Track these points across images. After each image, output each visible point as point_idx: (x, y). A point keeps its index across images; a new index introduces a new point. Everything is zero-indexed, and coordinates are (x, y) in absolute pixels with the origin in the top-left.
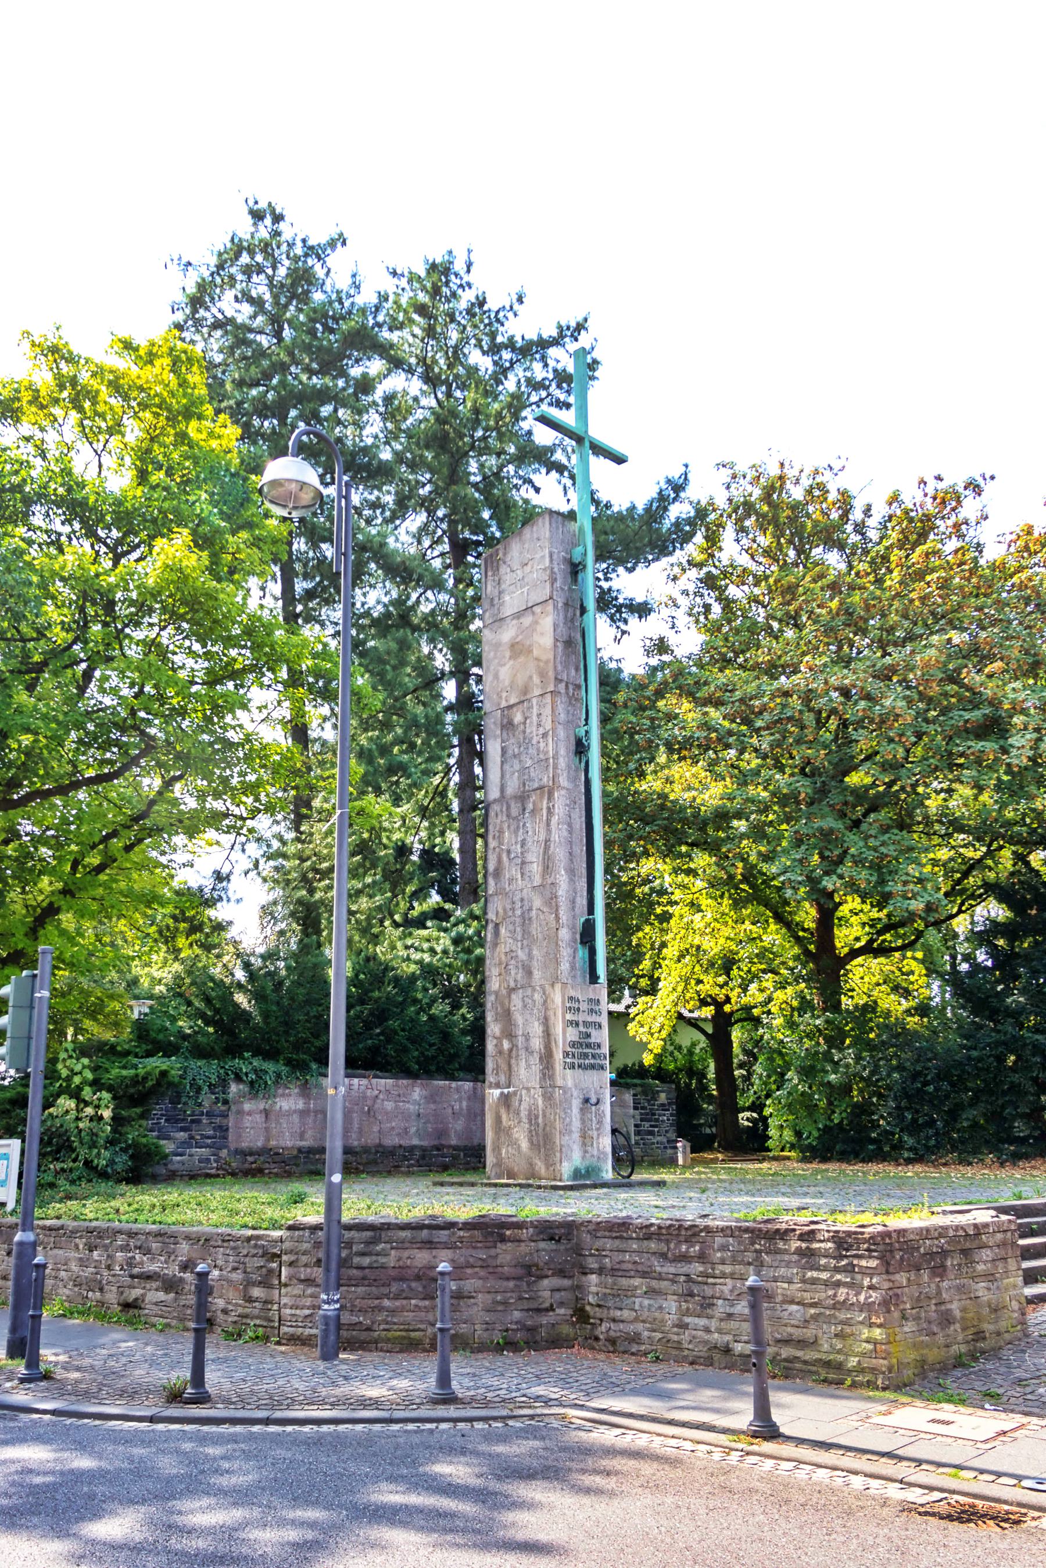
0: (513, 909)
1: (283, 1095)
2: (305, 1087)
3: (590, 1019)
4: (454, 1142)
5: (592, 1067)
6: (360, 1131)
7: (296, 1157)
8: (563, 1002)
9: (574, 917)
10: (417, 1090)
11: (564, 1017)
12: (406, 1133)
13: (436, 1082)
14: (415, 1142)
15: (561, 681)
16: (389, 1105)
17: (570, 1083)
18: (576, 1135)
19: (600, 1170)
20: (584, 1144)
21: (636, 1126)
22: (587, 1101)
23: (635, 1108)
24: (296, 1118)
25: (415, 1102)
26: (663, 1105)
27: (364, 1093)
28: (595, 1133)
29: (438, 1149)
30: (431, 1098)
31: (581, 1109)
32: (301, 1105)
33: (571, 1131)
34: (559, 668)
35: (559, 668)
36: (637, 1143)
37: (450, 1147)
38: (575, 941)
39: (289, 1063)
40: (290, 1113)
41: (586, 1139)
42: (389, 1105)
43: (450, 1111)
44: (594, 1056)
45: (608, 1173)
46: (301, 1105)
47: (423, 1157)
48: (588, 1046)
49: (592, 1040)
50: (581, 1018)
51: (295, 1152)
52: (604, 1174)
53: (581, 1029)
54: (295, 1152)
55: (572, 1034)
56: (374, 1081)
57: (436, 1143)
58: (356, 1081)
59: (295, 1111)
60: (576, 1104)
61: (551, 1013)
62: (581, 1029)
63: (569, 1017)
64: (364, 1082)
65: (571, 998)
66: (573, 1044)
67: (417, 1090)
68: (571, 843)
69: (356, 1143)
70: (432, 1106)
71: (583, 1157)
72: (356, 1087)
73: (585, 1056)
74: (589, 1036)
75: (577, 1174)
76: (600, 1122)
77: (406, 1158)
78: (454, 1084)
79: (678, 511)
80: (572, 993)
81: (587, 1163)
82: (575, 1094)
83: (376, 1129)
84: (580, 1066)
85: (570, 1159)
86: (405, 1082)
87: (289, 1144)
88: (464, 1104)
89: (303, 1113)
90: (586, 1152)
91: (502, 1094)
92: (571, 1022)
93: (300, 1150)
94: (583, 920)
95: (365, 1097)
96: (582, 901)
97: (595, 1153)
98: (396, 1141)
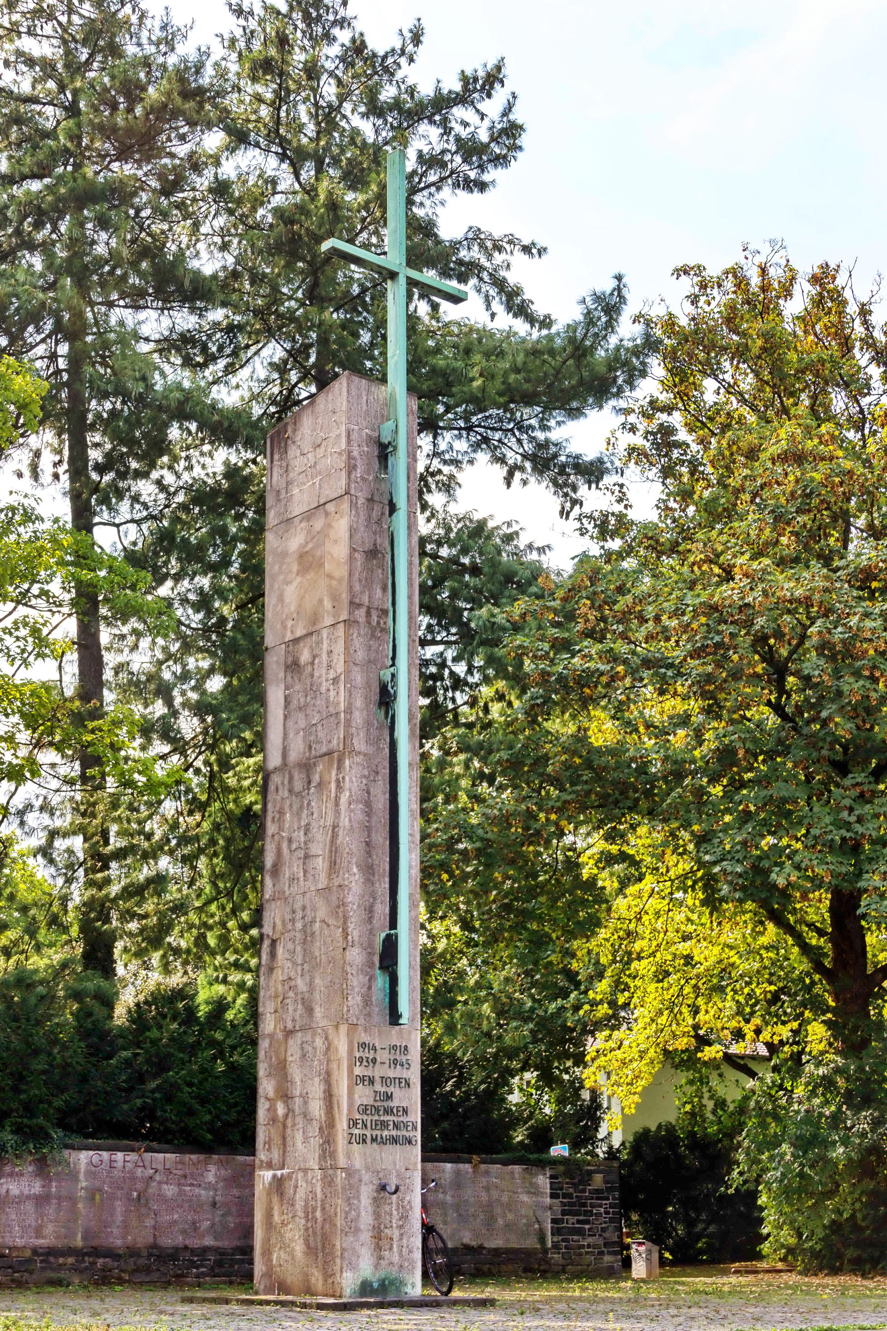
0: (293, 921)
1: (11, 1175)
2: (42, 1164)
3: (391, 1074)
5: (394, 1140)
6: (126, 1225)
7: (29, 1261)
8: (350, 1051)
9: (371, 932)
10: (213, 1168)
11: (350, 1071)
12: (196, 1229)
14: (209, 1241)
15: (359, 606)
16: (170, 1190)
17: (358, 1163)
18: (366, 1236)
19: (402, 1283)
20: (378, 1248)
21: (554, 1221)
22: (383, 1188)
23: (553, 1196)
24: (29, 1207)
25: (209, 1186)
26: (597, 1191)
27: (131, 1172)
28: (396, 1234)
31: (375, 1199)
32: (37, 1188)
33: (357, 1230)
34: (357, 587)
35: (357, 587)
36: (556, 1246)
38: (371, 965)
39: (18, 1130)
40: (21, 1199)
41: (379, 1239)
42: (170, 1190)
44: (396, 1126)
45: (415, 1287)
46: (37, 1188)
47: (219, 1264)
48: (388, 1111)
49: (395, 1103)
50: (378, 1072)
51: (28, 1253)
52: (409, 1289)
53: (378, 1087)
54: (28, 1253)
55: (364, 1095)
56: (148, 1156)
58: (120, 1156)
59: (28, 1197)
60: (366, 1194)
61: (334, 1066)
62: (378, 1087)
63: (358, 1071)
64: (133, 1157)
65: (363, 1045)
66: (365, 1109)
67: (213, 1168)
68: (369, 829)
69: (119, 1242)
70: (235, 1192)
71: (377, 1266)
72: (120, 1164)
73: (384, 1125)
74: (389, 1097)
75: (365, 1288)
76: (404, 1217)
77: (193, 1265)
79: (627, 331)
80: (365, 1038)
81: (382, 1274)
82: (366, 1177)
83: (149, 1222)
84: (374, 1140)
85: (353, 1267)
86: (194, 1157)
87: (19, 1242)
89: (41, 1200)
90: (380, 1258)
91: (274, 1176)
92: (363, 1079)
93: (35, 1251)
94: (383, 935)
95: (133, 1178)
96: (382, 909)
97: (396, 1259)
98: (180, 1240)
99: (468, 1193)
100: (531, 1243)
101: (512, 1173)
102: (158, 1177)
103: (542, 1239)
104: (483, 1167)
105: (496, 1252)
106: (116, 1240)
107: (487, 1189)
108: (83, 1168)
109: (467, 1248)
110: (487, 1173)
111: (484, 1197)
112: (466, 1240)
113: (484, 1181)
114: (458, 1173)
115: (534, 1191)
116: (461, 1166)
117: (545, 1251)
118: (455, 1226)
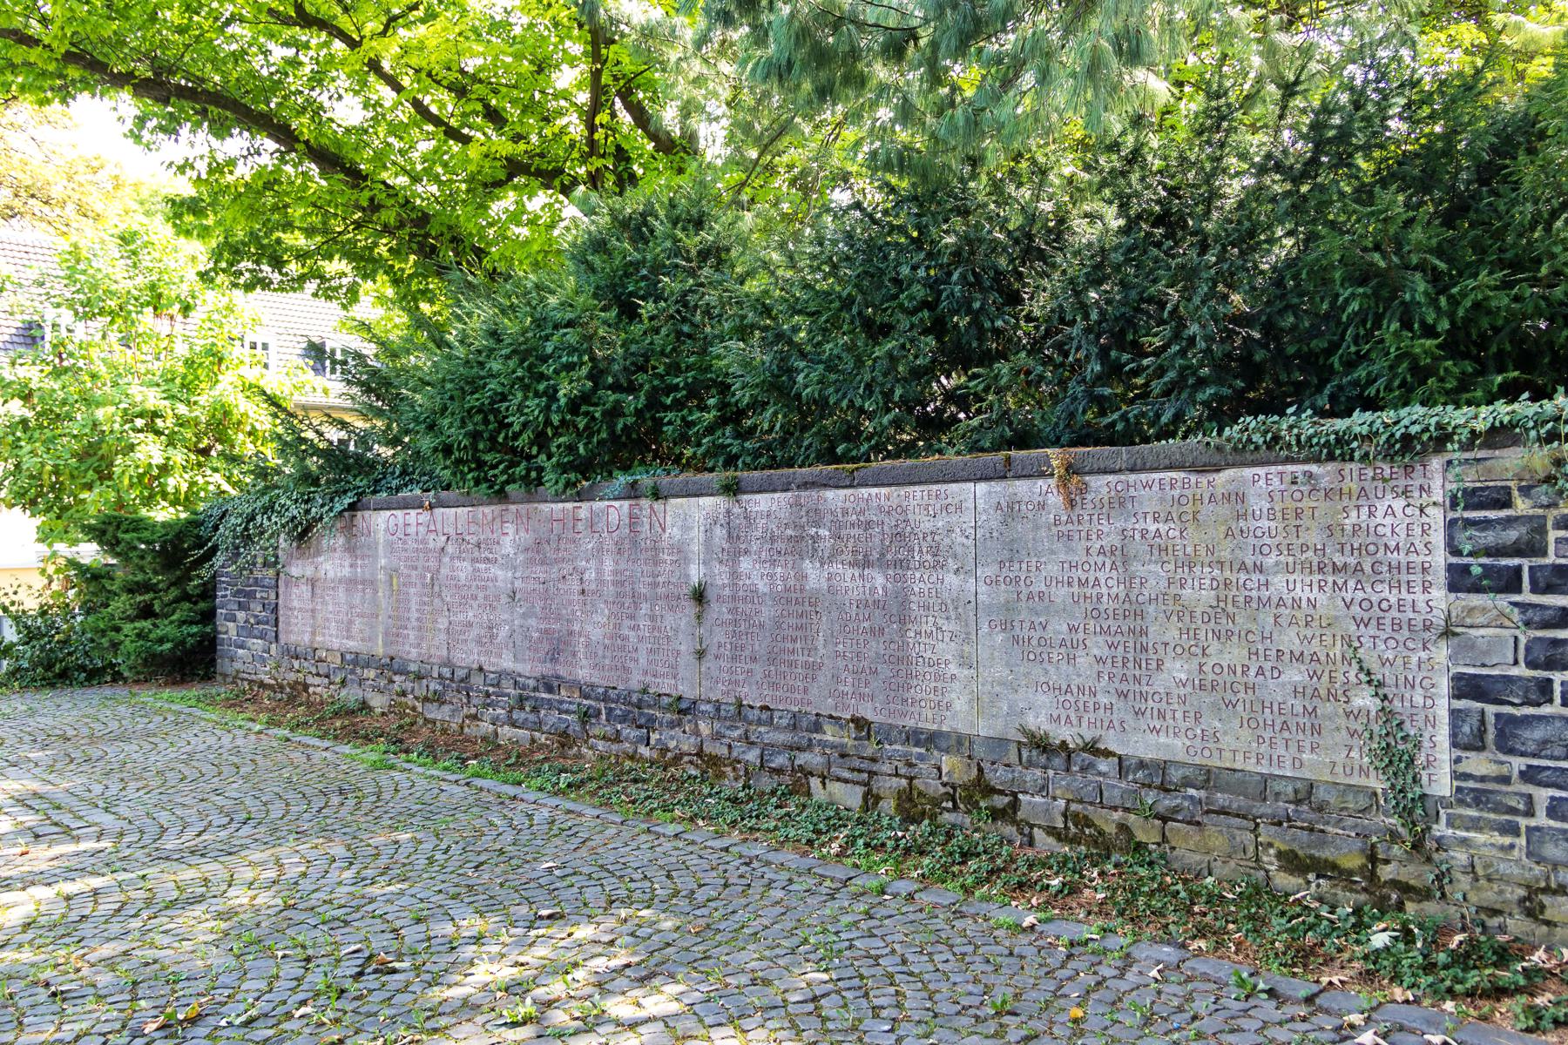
4: (583, 673)
10: (510, 528)
13: (546, 508)
14: (507, 663)
16: (464, 570)
21: (1466, 687)
23: (1459, 580)
29: (550, 689)
30: (537, 551)
32: (346, 571)
36: (1475, 794)
37: (576, 685)
43: (576, 587)
57: (547, 669)
67: (510, 528)
70: (540, 572)
78: (584, 509)
86: (487, 510)
87: (336, 643)
88: (609, 565)
99: (1049, 571)
100: (1338, 760)
101: (1238, 496)
102: (450, 549)
103: (1398, 757)
104: (1100, 485)
105: (1157, 775)
106: (411, 652)
107: (1121, 556)
108: (381, 537)
109: (1041, 745)
110: (1120, 502)
111: (1109, 584)
112: (1038, 722)
113: (1110, 531)
114: (1010, 511)
115: (1354, 561)
116: (1021, 487)
117: (1416, 809)
118: (1000, 671)
